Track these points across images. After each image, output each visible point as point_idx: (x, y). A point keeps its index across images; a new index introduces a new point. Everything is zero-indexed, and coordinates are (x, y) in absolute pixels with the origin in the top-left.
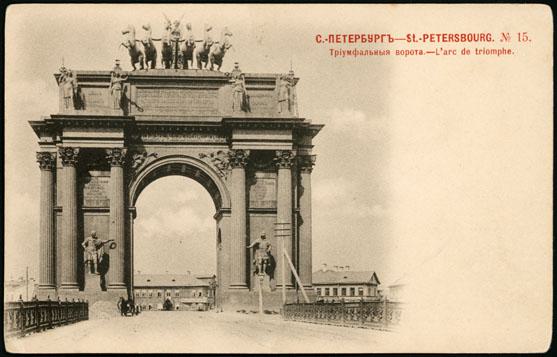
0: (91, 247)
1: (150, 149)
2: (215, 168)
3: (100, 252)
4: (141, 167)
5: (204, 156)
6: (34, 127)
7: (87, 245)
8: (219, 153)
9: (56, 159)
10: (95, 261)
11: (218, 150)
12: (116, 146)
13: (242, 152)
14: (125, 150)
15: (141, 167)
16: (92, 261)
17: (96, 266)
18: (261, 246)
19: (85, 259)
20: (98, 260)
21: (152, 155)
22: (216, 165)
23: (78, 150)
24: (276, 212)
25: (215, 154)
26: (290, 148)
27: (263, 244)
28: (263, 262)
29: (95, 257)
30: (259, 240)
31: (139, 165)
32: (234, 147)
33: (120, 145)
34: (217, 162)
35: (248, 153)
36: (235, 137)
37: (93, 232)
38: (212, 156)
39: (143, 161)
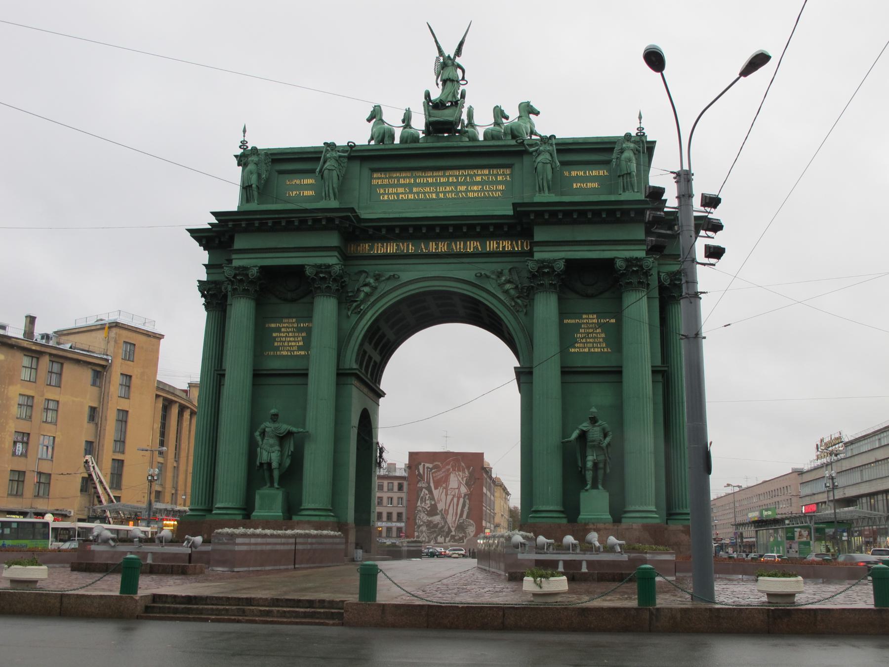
1: (387, 268)
2: (502, 297)
3: (290, 447)
4: (372, 299)
5: (480, 276)
7: (263, 434)
9: (227, 292)
10: (275, 465)
11: (510, 266)
14: (337, 268)
15: (372, 299)
16: (269, 464)
17: (276, 474)
20: (280, 464)
22: (506, 292)
26: (642, 254)
27: (595, 433)
28: (595, 465)
29: (275, 458)
30: (585, 426)
31: (368, 295)
32: (538, 256)
33: (332, 260)
34: (508, 286)
35: (561, 265)
36: (537, 238)
37: (273, 411)
39: (375, 288)
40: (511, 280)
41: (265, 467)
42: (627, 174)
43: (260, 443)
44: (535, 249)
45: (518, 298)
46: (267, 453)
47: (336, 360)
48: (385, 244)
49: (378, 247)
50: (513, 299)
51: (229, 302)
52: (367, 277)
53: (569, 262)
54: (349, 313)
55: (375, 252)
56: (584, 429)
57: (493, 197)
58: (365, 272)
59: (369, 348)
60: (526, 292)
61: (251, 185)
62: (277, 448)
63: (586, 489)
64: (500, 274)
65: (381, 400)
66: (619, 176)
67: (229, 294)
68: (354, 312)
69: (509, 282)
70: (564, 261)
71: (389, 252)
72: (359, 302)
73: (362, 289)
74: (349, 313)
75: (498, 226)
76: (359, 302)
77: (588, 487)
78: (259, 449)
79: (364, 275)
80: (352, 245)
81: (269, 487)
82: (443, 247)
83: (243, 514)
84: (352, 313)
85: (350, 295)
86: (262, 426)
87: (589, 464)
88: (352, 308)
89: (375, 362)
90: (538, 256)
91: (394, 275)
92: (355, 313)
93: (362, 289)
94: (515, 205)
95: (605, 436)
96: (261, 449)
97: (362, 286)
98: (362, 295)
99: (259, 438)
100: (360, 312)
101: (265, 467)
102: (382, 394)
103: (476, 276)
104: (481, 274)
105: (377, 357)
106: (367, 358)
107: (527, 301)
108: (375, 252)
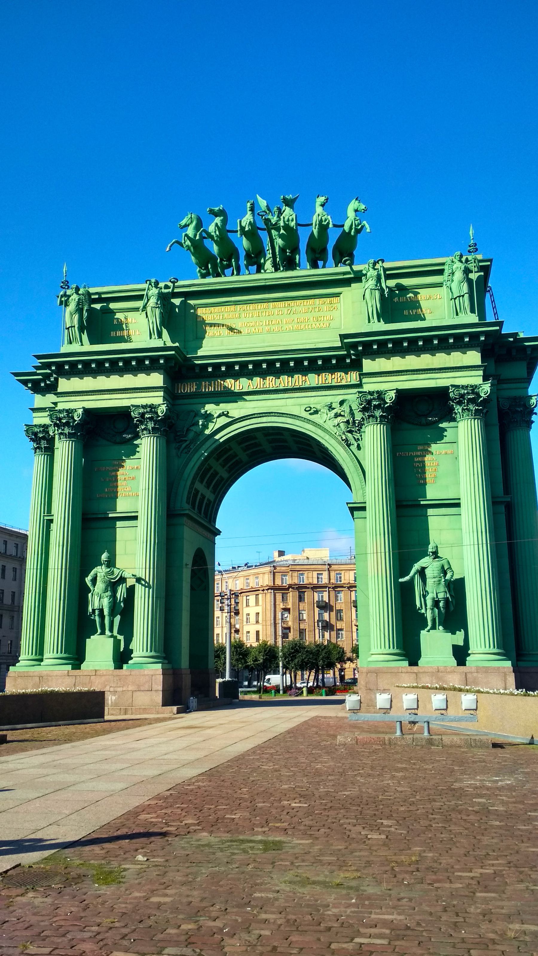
0: (100, 586)
3: (121, 592)
4: (202, 438)
6: (25, 383)
8: (342, 403)
11: (341, 398)
12: (149, 401)
13: (380, 395)
16: (101, 611)
18: (428, 573)
19: (90, 609)
21: (219, 416)
23: (80, 411)
24: (458, 505)
25: (336, 405)
28: (436, 603)
29: (106, 602)
38: (331, 408)
40: (342, 413)
41: (97, 612)
42: (459, 297)
43: (92, 588)
44: (364, 380)
45: (350, 432)
46: (99, 598)
47: (166, 501)
48: (213, 382)
49: (205, 386)
50: (344, 433)
51: (56, 447)
52: (195, 416)
53: (400, 393)
54: (179, 454)
55: (203, 391)
56: (424, 566)
57: (321, 329)
58: (194, 411)
59: (200, 487)
60: (358, 427)
61: (74, 327)
62: (109, 593)
63: (426, 630)
64: (331, 408)
65: (217, 538)
66: (451, 299)
67: (57, 437)
68: (184, 452)
69: (340, 415)
70: (395, 391)
71: (216, 389)
72: (188, 442)
73: (191, 428)
74: (179, 454)
75: (327, 360)
76: (188, 442)
77: (429, 628)
78: (90, 595)
79: (193, 414)
80: (180, 384)
81: (101, 634)
82: (270, 382)
83: (72, 665)
84: (181, 453)
85: (178, 434)
86: (92, 573)
87: (429, 603)
88: (181, 449)
89: (208, 500)
90: (366, 388)
91: (223, 413)
92: (186, 453)
93: (191, 428)
94: (343, 337)
95: (445, 573)
96: (92, 594)
97: (191, 426)
98: (191, 435)
99: (89, 584)
100: (189, 451)
101: (97, 612)
102: (217, 532)
103: (305, 410)
104: (311, 408)
105: (209, 495)
106: (199, 496)
107: (358, 435)
108: (203, 391)
